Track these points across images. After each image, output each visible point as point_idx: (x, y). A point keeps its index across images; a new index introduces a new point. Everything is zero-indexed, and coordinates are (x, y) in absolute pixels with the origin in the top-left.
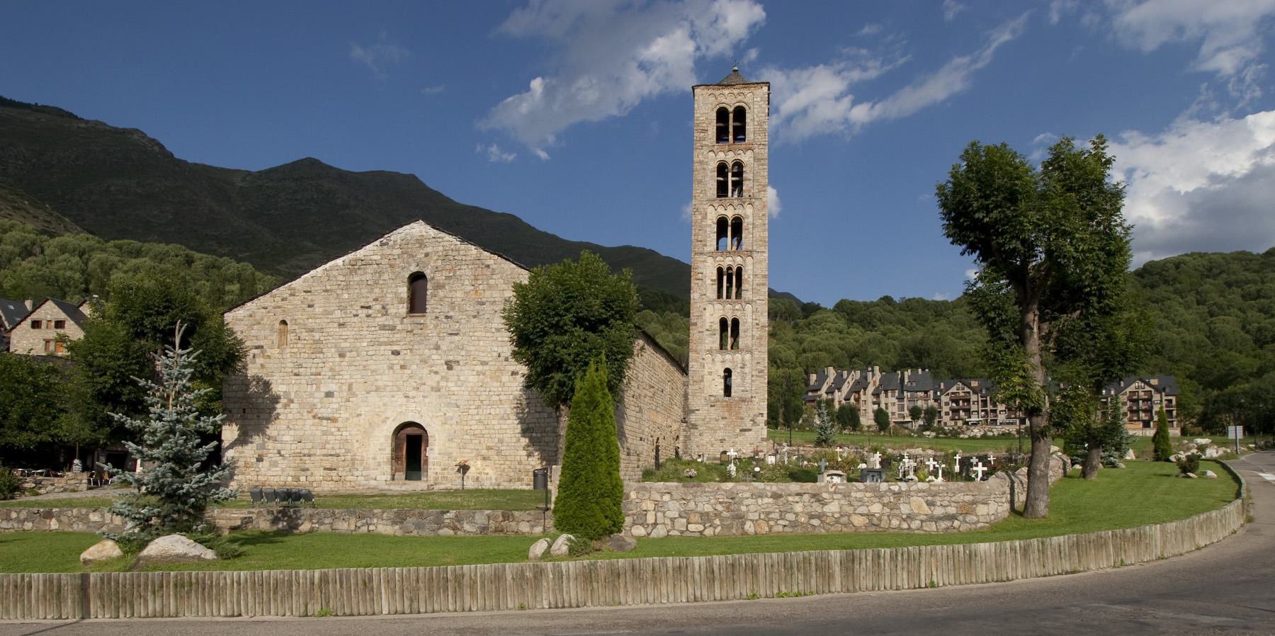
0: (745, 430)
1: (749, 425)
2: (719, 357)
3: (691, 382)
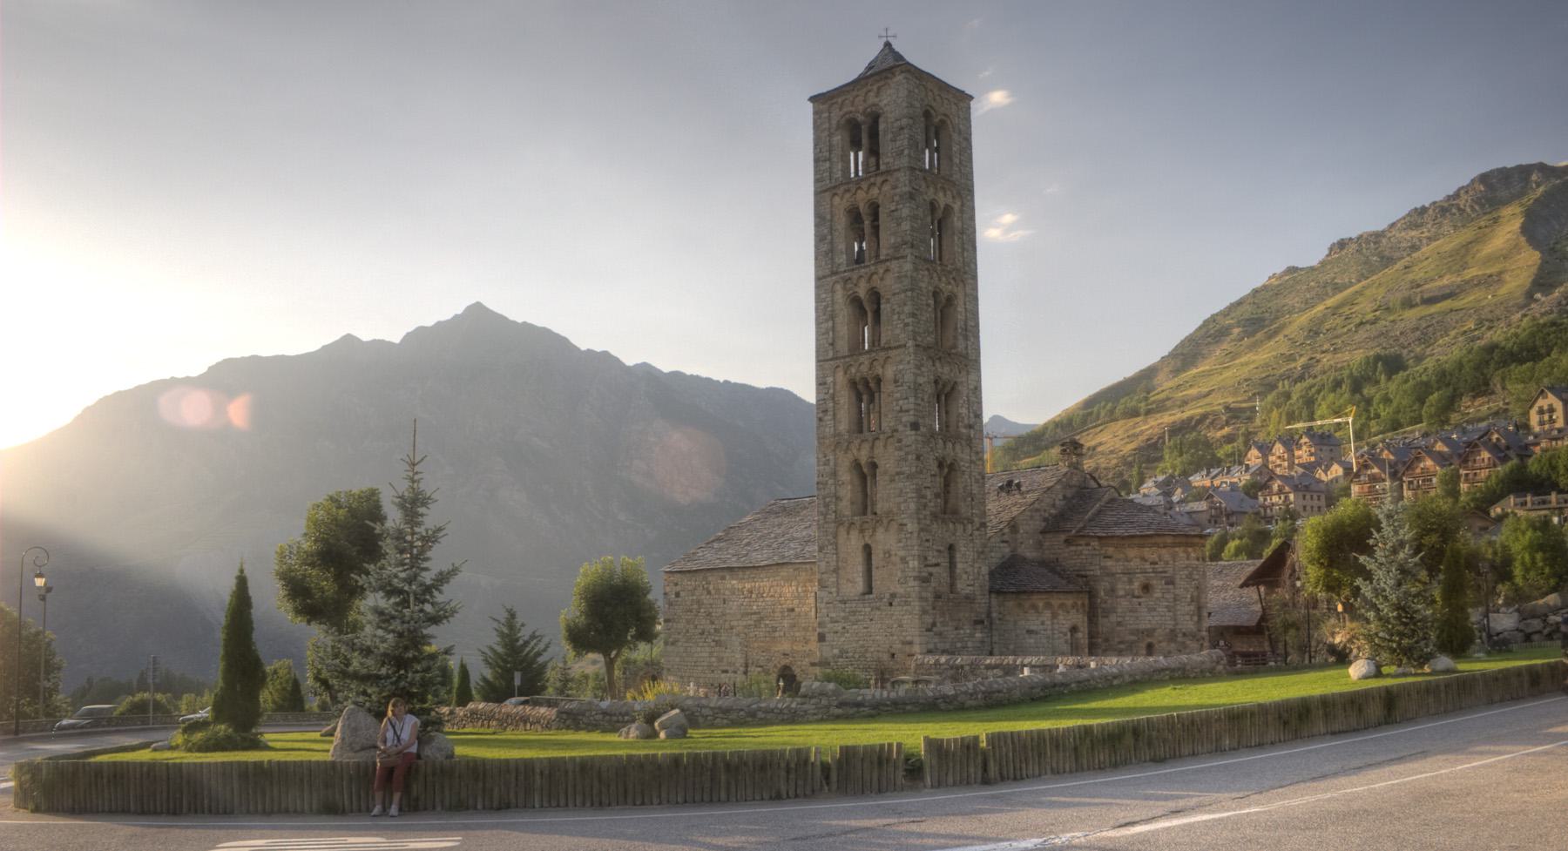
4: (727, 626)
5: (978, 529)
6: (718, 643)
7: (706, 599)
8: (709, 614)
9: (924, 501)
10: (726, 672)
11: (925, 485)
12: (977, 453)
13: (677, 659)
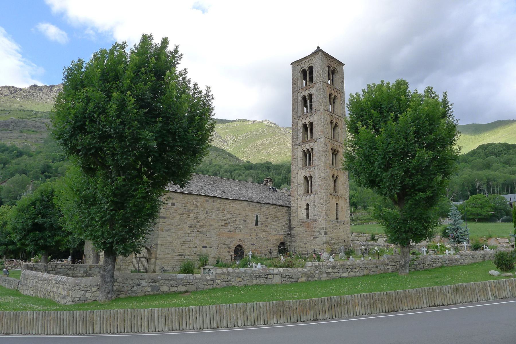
0: (314, 238)
1: (317, 235)
2: (304, 198)
3: (292, 213)
4: (208, 224)
6: (201, 233)
7: (194, 209)
8: (197, 217)
10: (206, 247)
13: (171, 239)
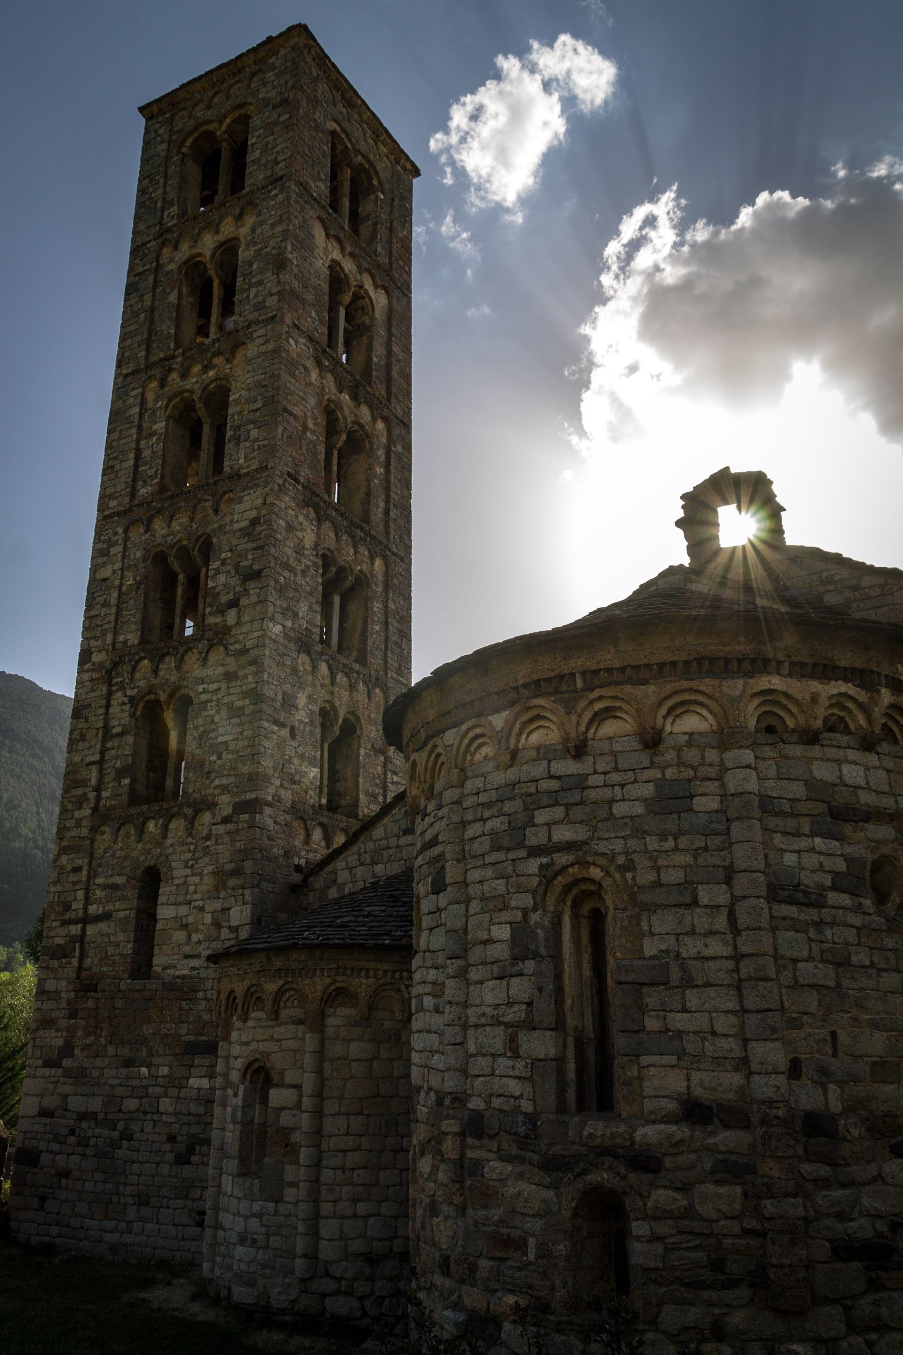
5: (225, 821)
9: (79, 792)
11: (90, 759)
12: (245, 651)
